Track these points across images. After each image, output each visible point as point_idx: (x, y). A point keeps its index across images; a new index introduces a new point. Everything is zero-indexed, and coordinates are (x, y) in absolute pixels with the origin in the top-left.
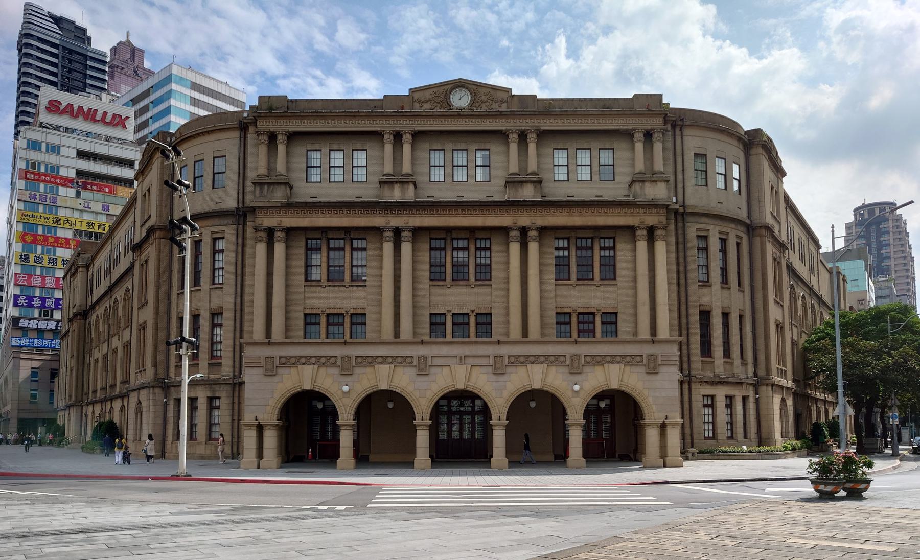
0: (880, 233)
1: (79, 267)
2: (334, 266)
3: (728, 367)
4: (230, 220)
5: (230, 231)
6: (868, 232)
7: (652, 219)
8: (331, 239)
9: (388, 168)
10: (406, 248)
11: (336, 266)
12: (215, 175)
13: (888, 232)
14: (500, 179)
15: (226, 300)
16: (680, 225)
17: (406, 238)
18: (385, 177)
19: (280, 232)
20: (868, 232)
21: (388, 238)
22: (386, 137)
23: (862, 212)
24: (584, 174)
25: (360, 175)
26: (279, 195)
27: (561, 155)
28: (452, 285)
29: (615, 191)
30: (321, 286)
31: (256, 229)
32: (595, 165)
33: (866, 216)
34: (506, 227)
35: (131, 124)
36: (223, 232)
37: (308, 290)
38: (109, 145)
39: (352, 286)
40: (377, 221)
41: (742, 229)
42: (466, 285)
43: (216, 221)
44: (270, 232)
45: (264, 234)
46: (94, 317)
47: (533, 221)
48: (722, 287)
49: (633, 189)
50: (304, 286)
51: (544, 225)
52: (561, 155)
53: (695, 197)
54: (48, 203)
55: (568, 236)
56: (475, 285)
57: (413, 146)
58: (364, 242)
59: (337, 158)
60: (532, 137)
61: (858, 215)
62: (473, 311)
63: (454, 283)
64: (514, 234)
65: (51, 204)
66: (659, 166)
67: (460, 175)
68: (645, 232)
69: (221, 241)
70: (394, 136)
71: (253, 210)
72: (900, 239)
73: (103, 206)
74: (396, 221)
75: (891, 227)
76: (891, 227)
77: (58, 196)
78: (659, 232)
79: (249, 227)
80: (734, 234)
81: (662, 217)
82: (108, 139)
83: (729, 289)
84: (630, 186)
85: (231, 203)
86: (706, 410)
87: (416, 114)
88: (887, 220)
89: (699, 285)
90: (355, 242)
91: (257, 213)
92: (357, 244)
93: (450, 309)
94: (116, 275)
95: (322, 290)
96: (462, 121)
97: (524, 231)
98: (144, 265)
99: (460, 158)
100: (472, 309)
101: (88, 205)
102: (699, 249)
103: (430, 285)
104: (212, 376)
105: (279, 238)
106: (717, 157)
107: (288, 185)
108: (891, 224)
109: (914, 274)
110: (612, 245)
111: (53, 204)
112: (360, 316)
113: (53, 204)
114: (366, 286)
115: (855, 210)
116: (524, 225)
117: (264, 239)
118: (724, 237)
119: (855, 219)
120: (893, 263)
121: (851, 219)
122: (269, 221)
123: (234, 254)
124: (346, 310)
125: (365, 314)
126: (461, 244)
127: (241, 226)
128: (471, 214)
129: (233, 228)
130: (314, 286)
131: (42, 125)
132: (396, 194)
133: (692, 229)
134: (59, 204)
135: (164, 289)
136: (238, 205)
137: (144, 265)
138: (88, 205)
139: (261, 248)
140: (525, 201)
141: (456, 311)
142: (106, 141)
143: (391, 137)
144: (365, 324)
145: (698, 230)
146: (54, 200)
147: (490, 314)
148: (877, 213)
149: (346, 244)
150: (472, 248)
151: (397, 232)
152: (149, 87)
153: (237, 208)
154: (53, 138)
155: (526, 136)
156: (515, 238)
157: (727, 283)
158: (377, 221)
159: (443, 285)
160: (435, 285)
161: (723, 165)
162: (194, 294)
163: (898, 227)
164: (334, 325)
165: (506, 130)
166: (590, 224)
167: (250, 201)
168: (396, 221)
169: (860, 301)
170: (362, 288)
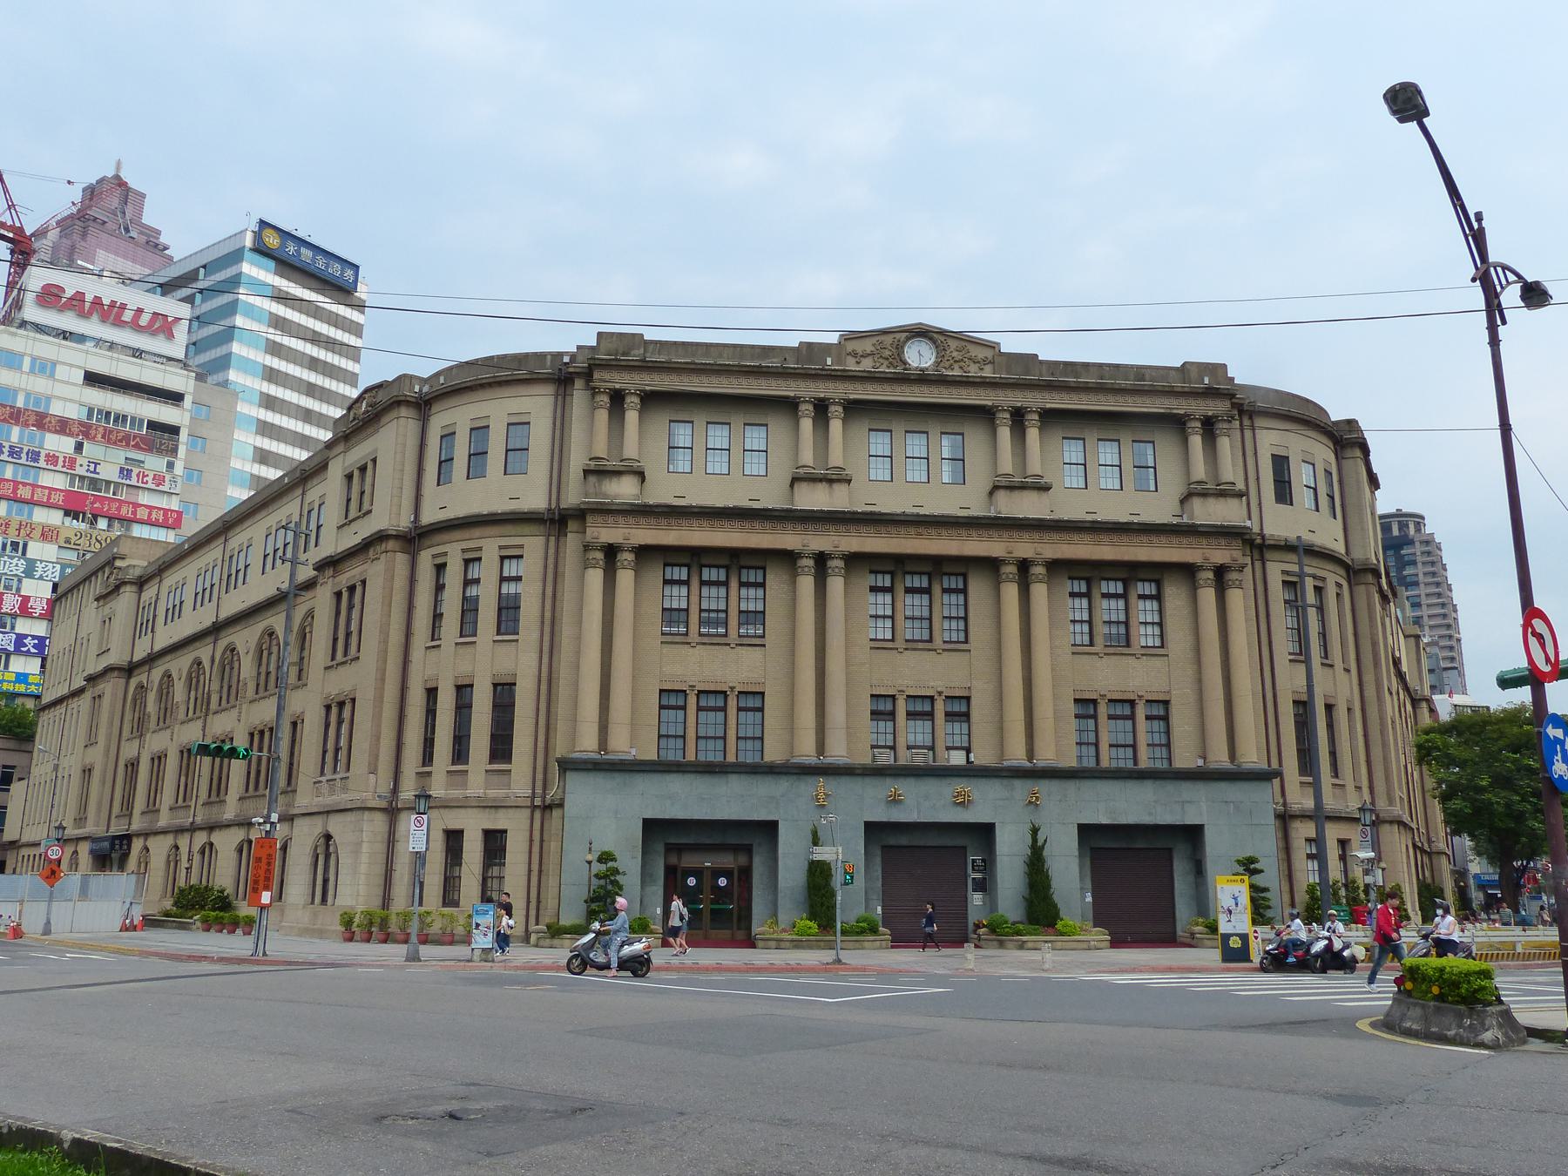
1: (124, 583)
2: (709, 611)
3: (1337, 791)
4: (533, 528)
5: (533, 544)
7: (1220, 556)
8: (706, 566)
9: (807, 457)
11: (713, 611)
12: (509, 452)
13: (1414, 563)
14: (979, 480)
15: (521, 661)
16: (1258, 564)
17: (837, 570)
18: (801, 470)
19: (627, 553)
21: (806, 569)
22: (803, 407)
24: (1109, 480)
26: (623, 490)
27: (1073, 449)
28: (906, 649)
29: (1160, 509)
30: (689, 643)
31: (587, 548)
32: (1128, 467)
34: (996, 559)
35: (181, 333)
36: (521, 546)
37: (667, 649)
38: (142, 365)
39: (741, 645)
41: (1342, 572)
42: (930, 650)
43: (509, 529)
44: (611, 551)
45: (600, 555)
46: (157, 673)
47: (1039, 550)
48: (1322, 664)
49: (1187, 506)
50: (662, 642)
51: (1055, 557)
52: (1073, 449)
53: (1279, 523)
54: (23, 461)
55: (1088, 575)
56: (944, 650)
57: (845, 421)
58: (760, 573)
62: (940, 693)
63: (910, 645)
64: (1010, 570)
65: (28, 463)
67: (917, 472)
68: (1210, 575)
69: (514, 562)
70: (815, 406)
71: (580, 515)
73: (122, 470)
74: (819, 541)
76: (1418, 553)
77: (41, 450)
78: (1233, 576)
79: (572, 542)
80: (1333, 577)
81: (1238, 552)
82: (138, 353)
83: (1331, 666)
84: (1182, 502)
85: (535, 498)
86: (1310, 863)
87: (851, 374)
88: (1411, 542)
89: (1290, 661)
90: (744, 572)
91: (589, 519)
92: (752, 576)
93: (905, 689)
94: (234, 603)
95: (691, 650)
96: (925, 389)
97: (1024, 566)
98: (345, 596)
99: (916, 445)
100: (939, 689)
101: (95, 468)
102: (1286, 602)
103: (871, 648)
104: (492, 793)
105: (626, 563)
106: (1303, 461)
107: (641, 475)
108: (1418, 549)
109: (1459, 633)
110: (1154, 593)
111: (32, 464)
112: (751, 696)
113: (32, 464)
114: (764, 646)
116: (1025, 557)
117: (601, 562)
118: (1320, 584)
123: (540, 584)
124: (731, 685)
125: (763, 694)
126: (917, 582)
127: (552, 539)
128: (939, 534)
129: (540, 541)
130: (677, 643)
131: (23, 324)
132: (814, 499)
134: (42, 463)
135: (396, 637)
136: (550, 504)
137: (345, 596)
138: (95, 468)
139: (595, 577)
142: (134, 356)
143: (811, 408)
144: (761, 710)
145: (1284, 572)
146: (35, 456)
147: (968, 699)
148: (1396, 532)
149: (692, 573)
150: (937, 590)
151: (821, 559)
152: (198, 266)
153: (549, 510)
154: (47, 348)
155: (1023, 416)
156: (1011, 576)
157: (1326, 657)
158: (787, 539)
159: (891, 649)
160: (878, 648)
161: (1312, 473)
162: (461, 650)
163: (1429, 553)
164: (707, 711)
165: (994, 407)
166: (1126, 558)
167: (573, 497)
168: (819, 541)
170: (757, 648)
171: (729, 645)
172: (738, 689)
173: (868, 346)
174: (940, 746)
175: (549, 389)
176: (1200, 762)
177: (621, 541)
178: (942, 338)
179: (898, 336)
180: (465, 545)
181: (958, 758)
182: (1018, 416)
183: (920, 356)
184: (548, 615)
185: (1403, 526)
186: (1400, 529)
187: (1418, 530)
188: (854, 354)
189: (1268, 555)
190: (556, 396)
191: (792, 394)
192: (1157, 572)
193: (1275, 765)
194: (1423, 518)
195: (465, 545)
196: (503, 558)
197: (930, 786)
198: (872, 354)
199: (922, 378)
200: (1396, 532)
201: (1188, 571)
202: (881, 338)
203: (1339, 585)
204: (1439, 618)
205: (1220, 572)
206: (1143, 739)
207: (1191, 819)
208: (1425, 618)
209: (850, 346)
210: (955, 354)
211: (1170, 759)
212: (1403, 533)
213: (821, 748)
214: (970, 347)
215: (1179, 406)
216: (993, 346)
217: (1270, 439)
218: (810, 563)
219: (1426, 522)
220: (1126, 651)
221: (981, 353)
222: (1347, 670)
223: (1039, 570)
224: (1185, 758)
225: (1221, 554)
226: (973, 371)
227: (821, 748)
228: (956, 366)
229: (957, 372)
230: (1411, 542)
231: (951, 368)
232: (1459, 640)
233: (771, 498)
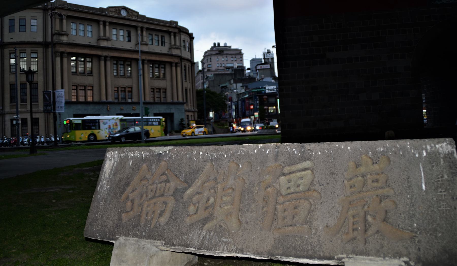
7: (177, 60)
9: (102, 34)
10: (108, 63)
25: (89, 35)
26: (64, 39)
36: (37, 50)
40: (99, 53)
41: (190, 63)
59: (81, 27)
60: (145, 29)
66: (178, 44)
71: (54, 44)
74: (105, 53)
78: (178, 65)
114: (93, 76)
122: (61, 49)
127: (45, 49)
133: (183, 63)
140: (144, 51)
141: (122, 86)
151: (106, 57)
158: (99, 53)
167: (49, 40)
168: (105, 53)
171: (85, 75)
172: (88, 85)
173: (113, 10)
174: (127, 97)
175: (41, 11)
176: (172, 101)
177: (64, 51)
178: (128, 10)
179: (120, 8)
180: (20, 49)
181: (130, 101)
182: (142, 28)
183: (124, 13)
184: (45, 67)
188: (111, 11)
189: (183, 60)
190: (43, 13)
191: (99, 19)
192: (164, 63)
193: (185, 101)
195: (20, 49)
196: (31, 53)
197: (128, 106)
198: (114, 12)
199: (124, 19)
201: (171, 63)
202: (116, 8)
203: (189, 65)
205: (176, 64)
206: (162, 96)
207: (172, 112)
209: (110, 9)
210: (130, 13)
211: (166, 100)
213: (107, 98)
214: (133, 12)
215: (171, 30)
216: (138, 13)
217: (183, 37)
218: (103, 58)
220: (159, 79)
221: (135, 14)
222: (190, 82)
223: (146, 62)
224: (169, 100)
225: (177, 60)
226: (134, 18)
227: (107, 98)
228: (131, 16)
229: (131, 18)
231: (130, 17)
233: (93, 42)
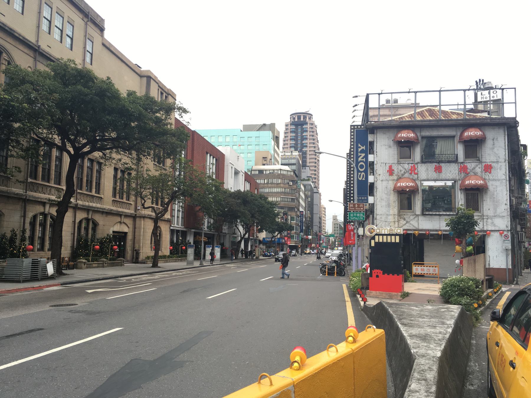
0: (304, 131)
6: (296, 129)
13: (307, 131)
20: (296, 129)
23: (294, 117)
33: (296, 120)
61: (292, 119)
72: (313, 136)
75: (309, 128)
76: (309, 128)
88: (306, 124)
108: (309, 126)
109: (319, 158)
115: (291, 115)
119: (291, 120)
120: (308, 149)
121: (288, 120)
148: (302, 119)
163: (312, 128)
169: (264, 158)
185: (305, 117)
186: (303, 118)
187: (310, 118)
194: (312, 115)
200: (302, 119)
204: (312, 152)
208: (308, 151)
212: (304, 120)
219: (313, 117)
230: (306, 124)
232: (318, 160)
